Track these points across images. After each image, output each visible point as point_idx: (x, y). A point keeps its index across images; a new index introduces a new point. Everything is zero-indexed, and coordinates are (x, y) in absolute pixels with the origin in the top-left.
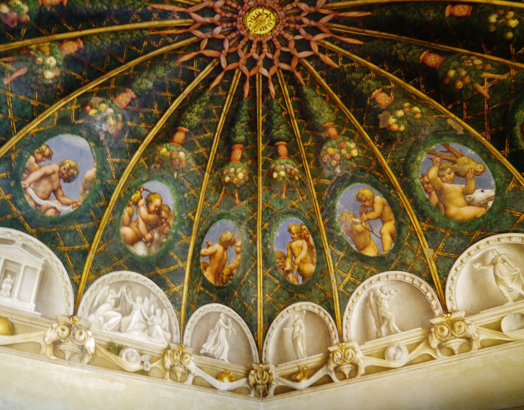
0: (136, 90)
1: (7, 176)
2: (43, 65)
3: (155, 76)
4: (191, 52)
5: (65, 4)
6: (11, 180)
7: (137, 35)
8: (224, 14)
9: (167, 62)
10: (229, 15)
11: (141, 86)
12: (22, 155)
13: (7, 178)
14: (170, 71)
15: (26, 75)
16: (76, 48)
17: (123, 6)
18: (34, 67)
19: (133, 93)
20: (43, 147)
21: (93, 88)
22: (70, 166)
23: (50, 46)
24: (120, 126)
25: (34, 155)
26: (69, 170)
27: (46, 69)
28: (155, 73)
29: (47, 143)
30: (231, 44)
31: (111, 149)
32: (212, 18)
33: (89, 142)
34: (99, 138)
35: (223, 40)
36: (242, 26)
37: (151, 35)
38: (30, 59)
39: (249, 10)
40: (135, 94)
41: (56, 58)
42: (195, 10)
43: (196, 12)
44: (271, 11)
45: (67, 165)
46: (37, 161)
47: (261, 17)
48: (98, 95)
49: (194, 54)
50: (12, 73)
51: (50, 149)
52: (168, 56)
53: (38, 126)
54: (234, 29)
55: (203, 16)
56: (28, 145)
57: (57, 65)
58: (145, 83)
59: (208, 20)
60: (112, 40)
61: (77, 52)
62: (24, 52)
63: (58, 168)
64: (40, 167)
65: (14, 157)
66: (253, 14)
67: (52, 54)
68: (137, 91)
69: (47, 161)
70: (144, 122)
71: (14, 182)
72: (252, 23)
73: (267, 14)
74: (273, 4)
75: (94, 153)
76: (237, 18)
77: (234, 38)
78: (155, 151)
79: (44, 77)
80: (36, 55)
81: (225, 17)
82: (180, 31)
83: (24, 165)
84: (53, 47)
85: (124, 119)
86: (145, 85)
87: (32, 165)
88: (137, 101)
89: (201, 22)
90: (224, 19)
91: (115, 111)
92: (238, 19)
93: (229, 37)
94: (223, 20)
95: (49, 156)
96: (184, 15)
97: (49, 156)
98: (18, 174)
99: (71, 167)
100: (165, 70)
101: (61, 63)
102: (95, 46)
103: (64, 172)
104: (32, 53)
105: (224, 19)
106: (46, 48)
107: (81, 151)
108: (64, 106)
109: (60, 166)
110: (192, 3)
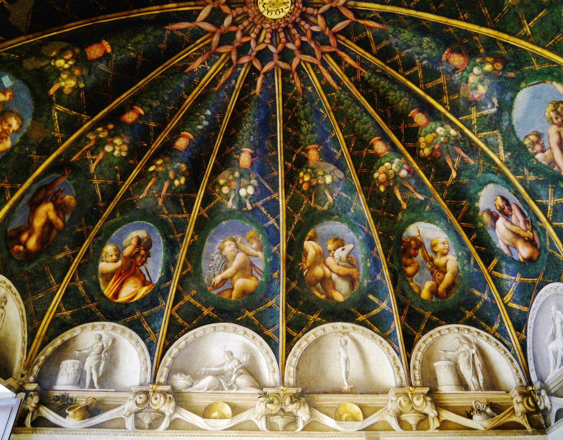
0: (440, 51)
1: (552, 187)
2: (448, 136)
3: (414, 38)
4: (363, 25)
5: (380, 137)
6: (557, 185)
7: (376, 79)
8: (297, 36)
9: (391, 36)
10: (294, 31)
11: (433, 47)
12: (533, 168)
13: (554, 188)
14: (399, 29)
15: (460, 148)
16: (420, 114)
17: (353, 104)
18: (451, 142)
19: (446, 52)
20: (527, 142)
21: (443, 105)
22: (553, 111)
23: (424, 136)
24: (489, 59)
25: (536, 154)
26: (558, 113)
27: (450, 134)
28: (411, 40)
29: (522, 139)
30: (320, 5)
31: (523, 65)
32: (309, 42)
33: (522, 89)
34: (513, 78)
35: (323, 15)
36: (294, 13)
37: (366, 70)
38: (445, 147)
39: (275, 20)
40: (446, 49)
41: (436, 128)
42: (313, 58)
43: (315, 57)
44: (257, 6)
45: (553, 115)
46: (543, 151)
47: (270, 9)
48: (458, 92)
49: (361, 22)
50: (462, 158)
51: (530, 135)
52: (382, 41)
53: (496, 152)
54: (304, 16)
55: (314, 50)
56: (520, 160)
57: (442, 126)
58: (428, 44)
59: (313, 45)
60: (395, 92)
61: (423, 113)
62: (438, 153)
63: (555, 126)
64: (550, 148)
65: (533, 177)
66: (274, 16)
67: (434, 131)
68: (441, 49)
69: (544, 139)
70: (472, 39)
71: (560, 182)
72: (284, 8)
73: (263, 6)
74: (251, 8)
75: (533, 83)
76: (291, 23)
77: (311, 7)
78: (514, 6)
79: (457, 136)
80: (439, 142)
81: (298, 33)
82: (343, 54)
83: (545, 166)
84: (425, 132)
85: (479, 57)
86: (430, 44)
87: (546, 157)
88: (454, 47)
89: (319, 50)
90: (301, 32)
91: (474, 66)
92: (290, 21)
93: (315, 12)
94: (302, 34)
95: (539, 136)
96: (325, 64)
97: (539, 136)
98: (554, 176)
99: (555, 110)
100: (402, 32)
101: (438, 124)
102: (410, 100)
103: (560, 120)
104: (437, 146)
105: (301, 32)
106: (429, 137)
107: (534, 97)
108: (470, 129)
109: (553, 123)
110: (309, 66)
